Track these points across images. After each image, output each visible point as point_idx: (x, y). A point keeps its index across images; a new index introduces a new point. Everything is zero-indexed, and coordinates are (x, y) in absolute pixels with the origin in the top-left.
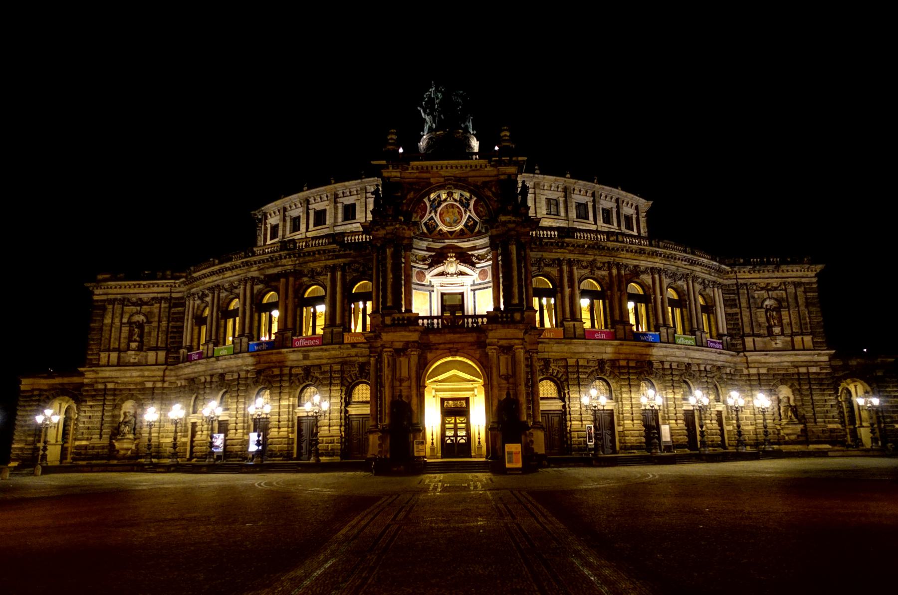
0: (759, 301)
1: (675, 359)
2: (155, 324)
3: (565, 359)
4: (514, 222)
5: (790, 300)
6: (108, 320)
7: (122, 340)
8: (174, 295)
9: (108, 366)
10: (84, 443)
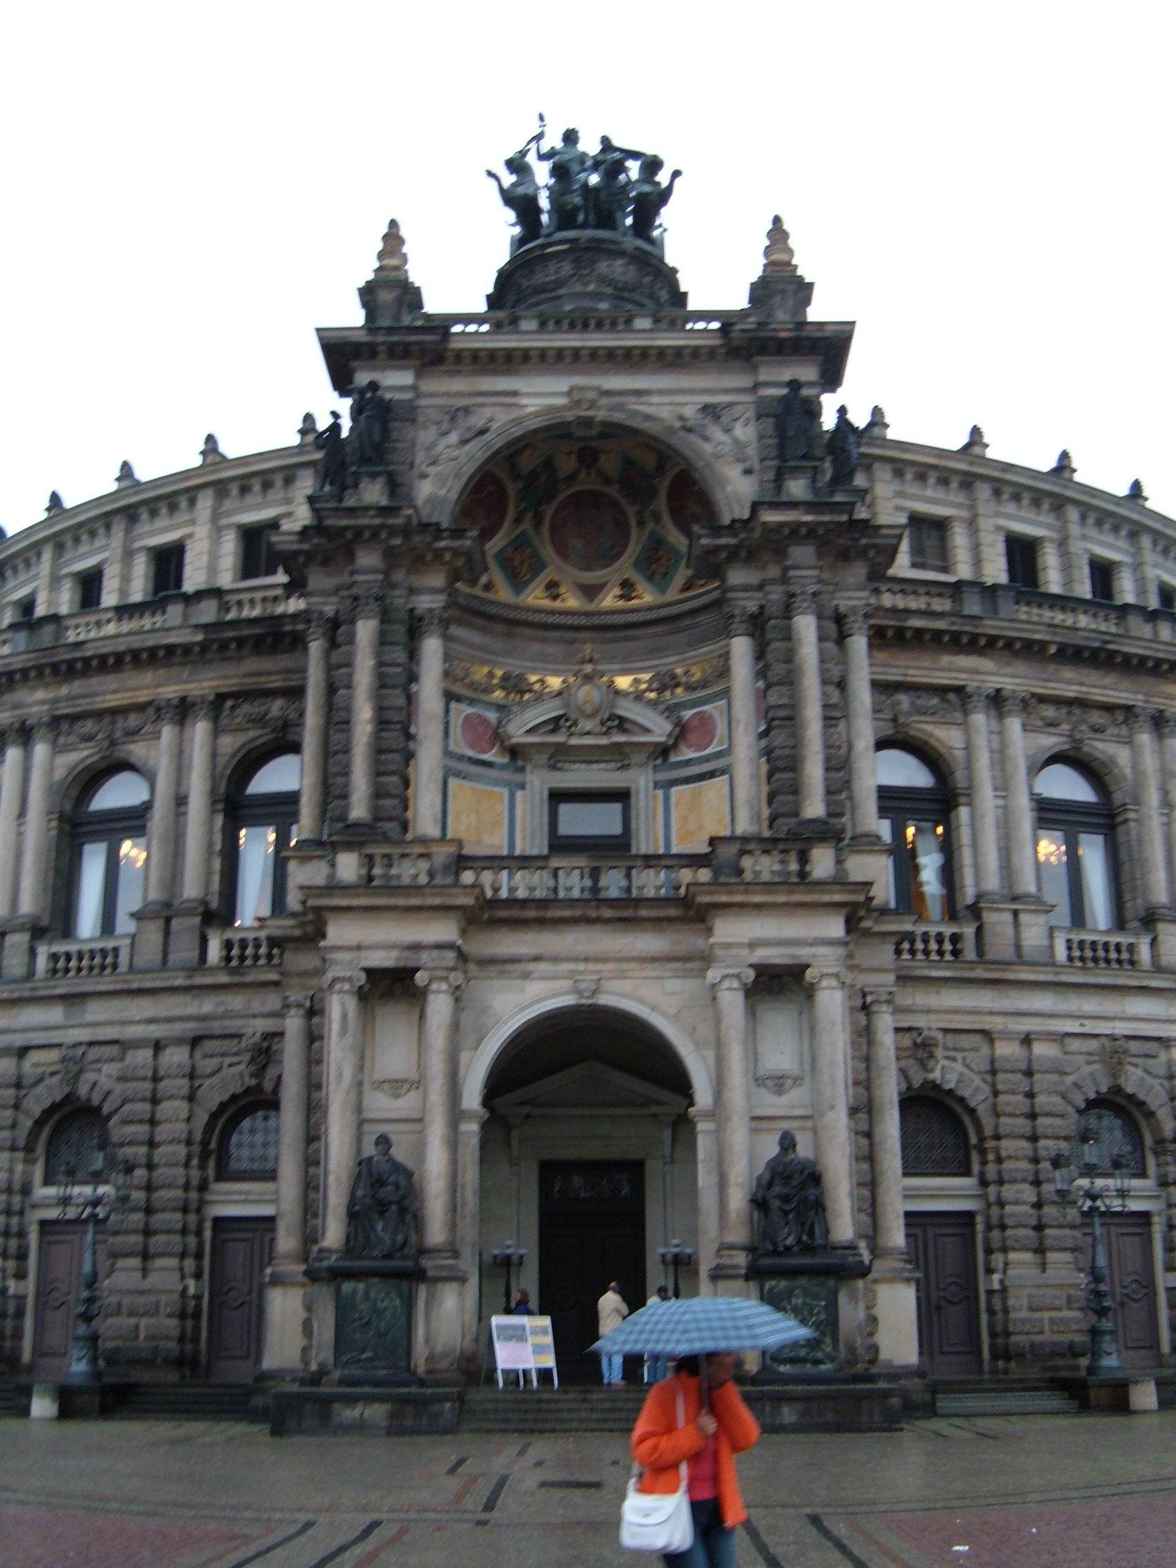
3: (987, 1035)
4: (812, 530)
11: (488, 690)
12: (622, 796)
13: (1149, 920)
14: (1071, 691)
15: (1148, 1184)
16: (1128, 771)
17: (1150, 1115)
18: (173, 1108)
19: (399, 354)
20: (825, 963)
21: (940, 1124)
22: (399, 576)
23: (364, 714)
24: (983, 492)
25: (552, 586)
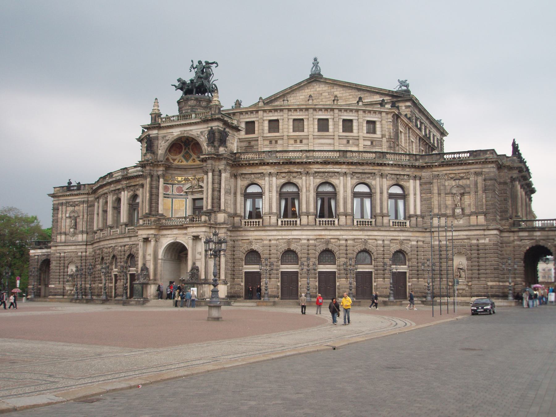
0: (448, 188)
1: (351, 237)
2: (81, 217)
4: (209, 158)
5: (471, 186)
6: (60, 216)
7: (67, 227)
8: (90, 199)
9: (61, 242)
10: (53, 286)
11: (182, 181)
16: (301, 185)
20: (202, 235)
21: (253, 256)
22: (155, 169)
25: (194, 159)
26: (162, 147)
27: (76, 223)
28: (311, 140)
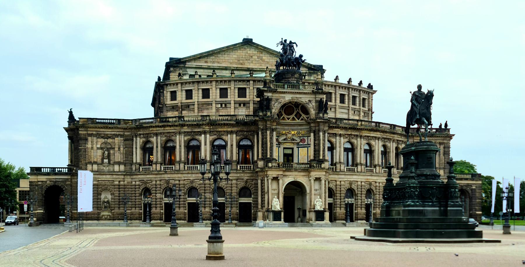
1: (381, 181)
2: (116, 149)
3: (336, 181)
6: (89, 145)
7: (98, 157)
8: (126, 133)
12: (292, 149)
13: (357, 165)
14: (350, 133)
15: (353, 200)
17: (355, 191)
18: (234, 189)
19: (270, 92)
23: (269, 144)
24: (338, 88)
25: (284, 117)
26: (275, 108)
27: (109, 154)
28: (337, 109)
